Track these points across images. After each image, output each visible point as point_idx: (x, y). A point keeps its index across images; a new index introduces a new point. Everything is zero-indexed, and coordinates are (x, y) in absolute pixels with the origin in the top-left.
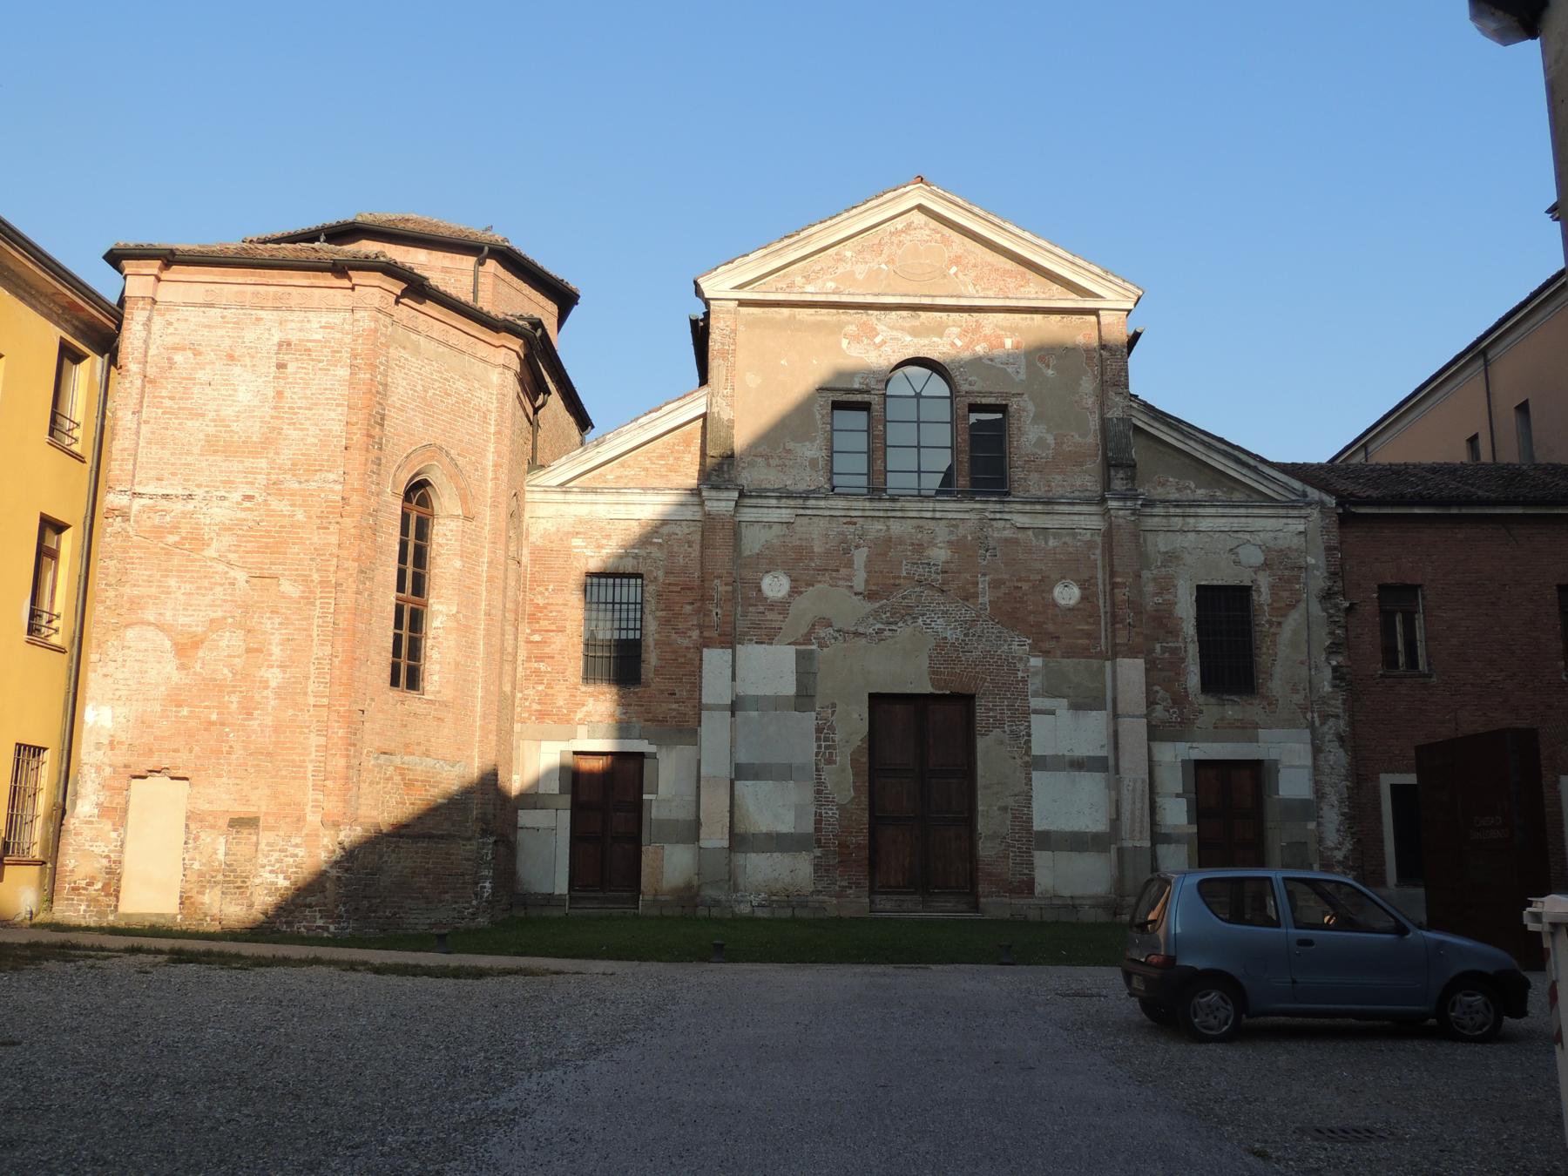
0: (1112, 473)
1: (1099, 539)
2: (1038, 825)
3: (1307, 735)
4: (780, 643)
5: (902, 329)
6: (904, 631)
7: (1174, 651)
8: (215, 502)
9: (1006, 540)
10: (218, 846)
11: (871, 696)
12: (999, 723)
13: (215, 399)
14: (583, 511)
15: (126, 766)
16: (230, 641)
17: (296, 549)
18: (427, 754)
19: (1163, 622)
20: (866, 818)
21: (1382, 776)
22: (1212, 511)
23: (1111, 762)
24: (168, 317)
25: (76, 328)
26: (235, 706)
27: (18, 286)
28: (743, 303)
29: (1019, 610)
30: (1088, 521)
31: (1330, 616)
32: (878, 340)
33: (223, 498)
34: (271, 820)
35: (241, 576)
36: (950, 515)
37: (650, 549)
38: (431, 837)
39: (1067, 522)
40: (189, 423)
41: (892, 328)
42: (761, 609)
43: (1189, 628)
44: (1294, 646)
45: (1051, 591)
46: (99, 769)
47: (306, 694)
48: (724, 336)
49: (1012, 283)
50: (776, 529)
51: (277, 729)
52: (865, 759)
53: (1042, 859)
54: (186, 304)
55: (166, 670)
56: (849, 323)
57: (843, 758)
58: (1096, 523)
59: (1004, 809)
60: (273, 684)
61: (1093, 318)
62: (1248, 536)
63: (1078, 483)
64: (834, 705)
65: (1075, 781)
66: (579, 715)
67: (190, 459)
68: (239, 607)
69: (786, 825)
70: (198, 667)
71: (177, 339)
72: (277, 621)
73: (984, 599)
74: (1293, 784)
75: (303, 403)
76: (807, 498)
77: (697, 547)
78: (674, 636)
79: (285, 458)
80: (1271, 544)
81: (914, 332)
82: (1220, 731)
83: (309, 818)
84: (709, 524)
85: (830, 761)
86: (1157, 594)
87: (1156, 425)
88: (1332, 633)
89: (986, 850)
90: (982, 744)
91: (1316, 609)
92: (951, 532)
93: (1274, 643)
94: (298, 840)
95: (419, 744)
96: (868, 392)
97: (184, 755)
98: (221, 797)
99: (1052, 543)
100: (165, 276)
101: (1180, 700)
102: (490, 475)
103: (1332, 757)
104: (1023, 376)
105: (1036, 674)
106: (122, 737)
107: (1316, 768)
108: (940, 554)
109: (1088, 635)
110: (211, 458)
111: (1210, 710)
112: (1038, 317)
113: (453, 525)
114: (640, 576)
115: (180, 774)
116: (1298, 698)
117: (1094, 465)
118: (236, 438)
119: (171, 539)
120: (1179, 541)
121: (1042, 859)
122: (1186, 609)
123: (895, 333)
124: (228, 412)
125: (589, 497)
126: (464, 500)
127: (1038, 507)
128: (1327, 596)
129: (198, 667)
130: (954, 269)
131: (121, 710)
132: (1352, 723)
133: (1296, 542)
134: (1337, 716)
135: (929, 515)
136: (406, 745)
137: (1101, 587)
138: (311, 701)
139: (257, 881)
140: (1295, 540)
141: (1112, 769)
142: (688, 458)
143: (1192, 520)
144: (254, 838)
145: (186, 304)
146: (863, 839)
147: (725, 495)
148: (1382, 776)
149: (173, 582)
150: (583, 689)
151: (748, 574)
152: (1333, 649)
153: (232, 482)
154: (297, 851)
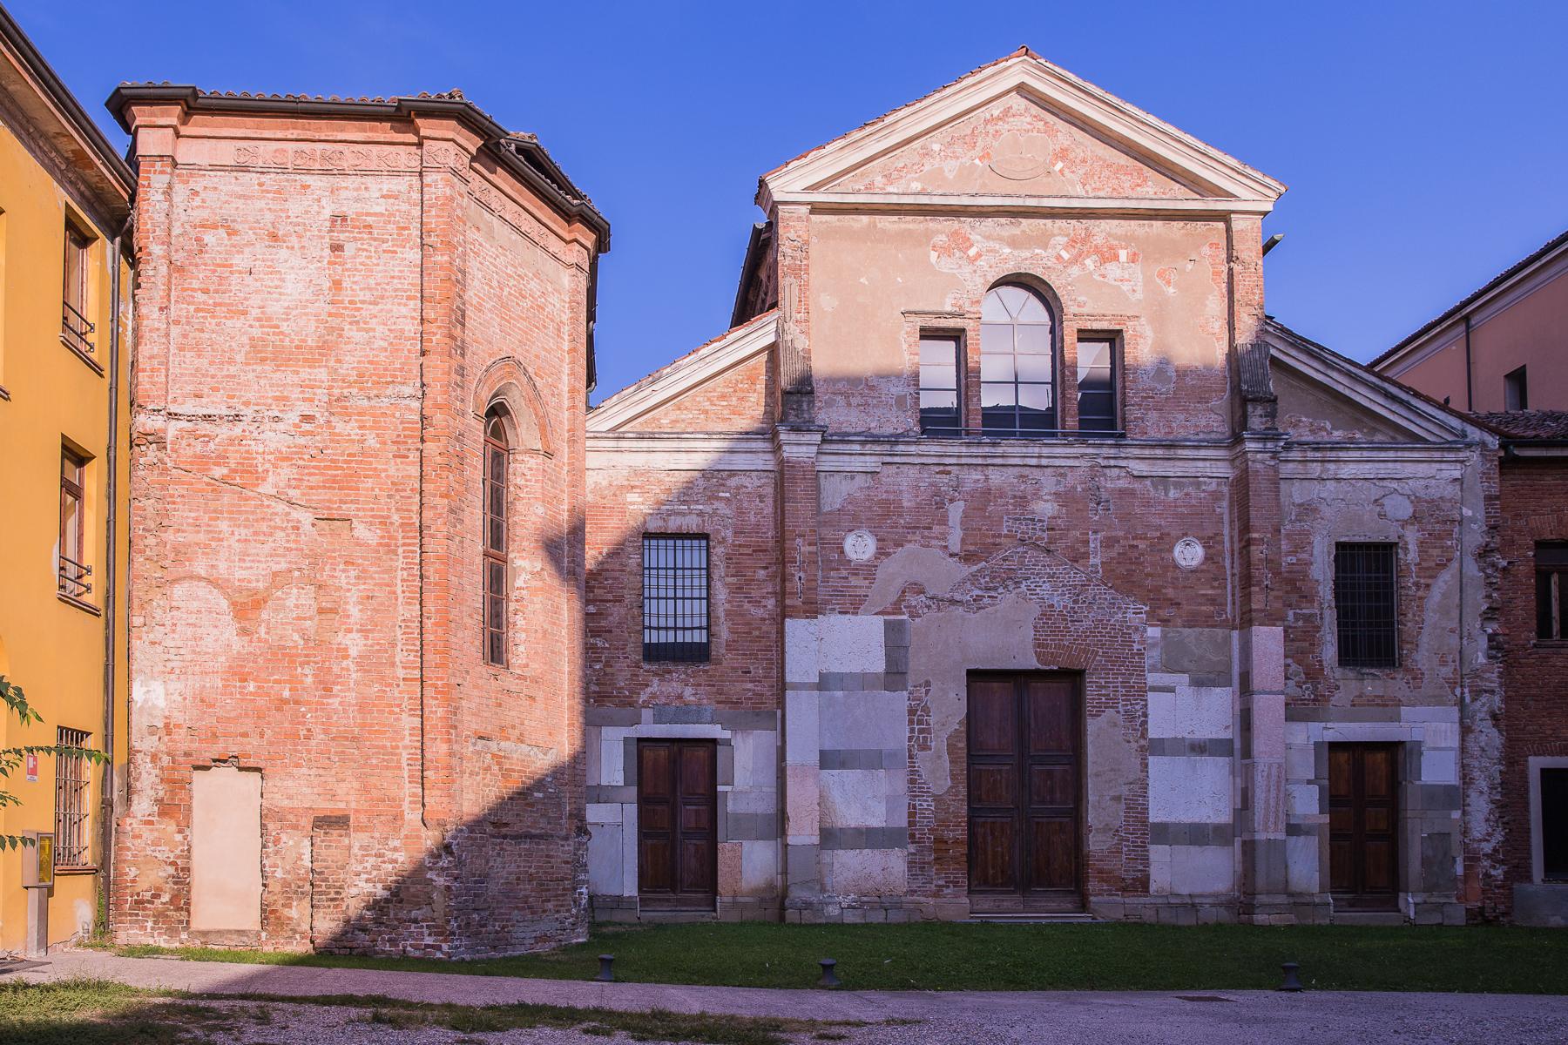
0: (1250, 408)
1: (1225, 489)
2: (1155, 817)
3: (1455, 713)
4: (866, 612)
5: (1000, 239)
6: (1007, 600)
7: (1308, 618)
8: (267, 425)
9: (1122, 492)
10: (297, 848)
11: (970, 673)
12: (1111, 703)
13: (257, 292)
14: (639, 460)
15: (186, 754)
16: (298, 599)
17: (370, 483)
18: (521, 740)
19: (1295, 586)
20: (964, 810)
21: (1531, 759)
22: (1356, 454)
23: (1237, 745)
24: (191, 185)
25: (82, 194)
26: (309, 680)
27: (14, 117)
28: (816, 209)
29: (1136, 574)
30: (1214, 468)
31: (1488, 577)
32: (972, 252)
33: (277, 419)
34: (363, 818)
35: (306, 518)
36: (1057, 462)
37: (717, 504)
38: (532, 837)
39: (1191, 469)
40: (229, 323)
41: (988, 238)
42: (844, 573)
43: (1326, 592)
44: (1447, 613)
45: (1171, 550)
46: (155, 758)
47: (393, 664)
48: (795, 249)
49: (1127, 182)
50: (860, 480)
51: (363, 707)
52: (963, 745)
53: (1158, 854)
54: (214, 168)
55: (222, 637)
56: (938, 232)
57: (939, 742)
58: (1223, 470)
59: (1117, 799)
60: (353, 652)
61: (1221, 225)
62: (1395, 485)
63: (1203, 423)
64: (928, 684)
65: (1197, 770)
66: (643, 697)
67: (233, 370)
68: (306, 556)
69: (876, 819)
70: (263, 630)
71: (205, 214)
72: (353, 574)
73: (1095, 560)
74: (1437, 768)
75: (367, 296)
76: (897, 443)
77: (770, 501)
78: (747, 606)
79: (348, 367)
80: (1421, 494)
81: (1013, 243)
82: (1359, 708)
83: (407, 817)
84: (783, 476)
85: (924, 747)
86: (1289, 553)
87: (1293, 352)
88: (1489, 596)
89: (1096, 843)
90: (1093, 726)
91: (1472, 569)
92: (1059, 482)
93: (1421, 608)
94: (397, 843)
95: (513, 727)
96: (961, 315)
97: (255, 741)
98: (300, 790)
99: (1172, 493)
100: (184, 130)
101: (1313, 674)
102: (566, 403)
103: (1483, 738)
104: (1139, 295)
105: (1154, 645)
106: (178, 717)
107: (1463, 749)
108: (1045, 508)
109: (1212, 601)
110: (259, 368)
111: (1349, 685)
112: (1158, 225)
113: (533, 462)
114: (706, 537)
115: (252, 763)
116: (1447, 671)
117: (1220, 401)
118: (287, 343)
119: (219, 472)
120: (1316, 490)
121: (1158, 854)
122: (1322, 571)
123: (991, 244)
124: (275, 309)
125: (645, 444)
126: (543, 429)
127: (1159, 452)
128: (1484, 553)
129: (263, 630)
130: (1059, 165)
131: (176, 686)
132: (1507, 700)
133: (1452, 491)
134: (1492, 692)
135: (1034, 462)
136: (502, 729)
137: (1227, 544)
138: (401, 673)
139: (354, 891)
140: (1450, 488)
141: (1237, 754)
142: (753, 398)
143: (1332, 466)
144: (347, 841)
145: (214, 168)
146: (961, 833)
147: (807, 438)
148: (1531, 759)
149: (224, 526)
150: (646, 667)
151: (827, 533)
152: (1490, 614)
153: (286, 399)
154: (395, 855)
